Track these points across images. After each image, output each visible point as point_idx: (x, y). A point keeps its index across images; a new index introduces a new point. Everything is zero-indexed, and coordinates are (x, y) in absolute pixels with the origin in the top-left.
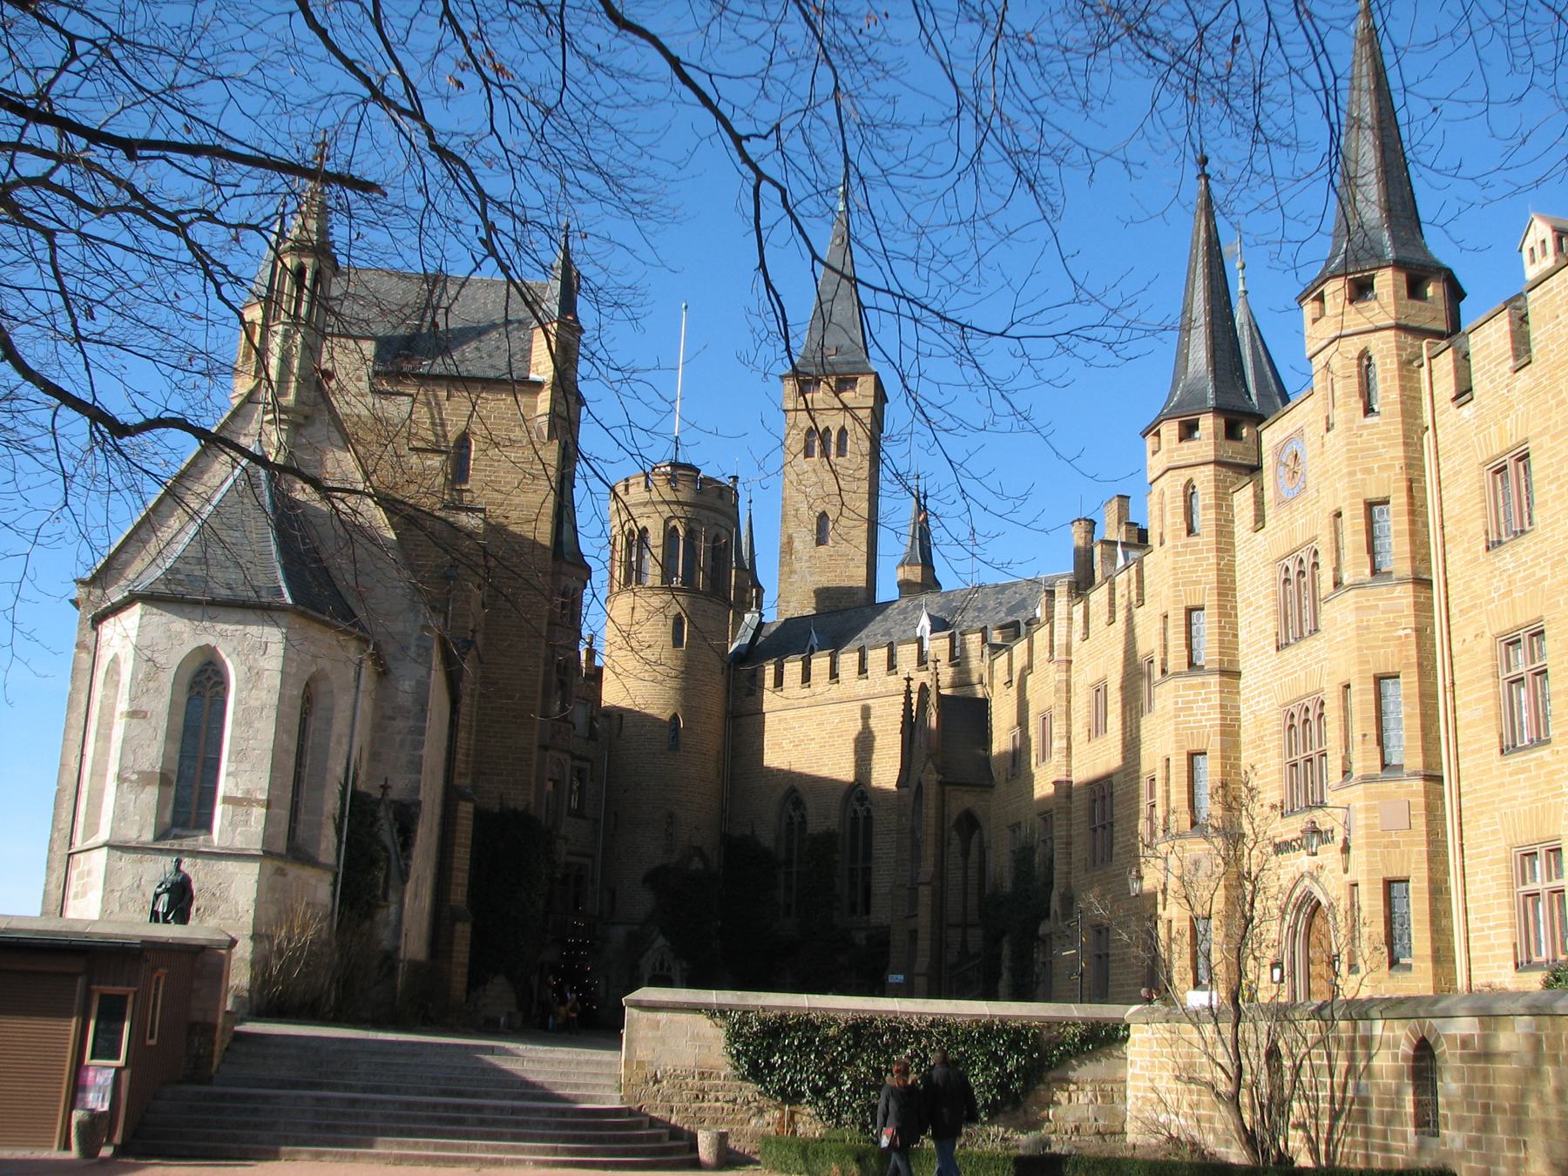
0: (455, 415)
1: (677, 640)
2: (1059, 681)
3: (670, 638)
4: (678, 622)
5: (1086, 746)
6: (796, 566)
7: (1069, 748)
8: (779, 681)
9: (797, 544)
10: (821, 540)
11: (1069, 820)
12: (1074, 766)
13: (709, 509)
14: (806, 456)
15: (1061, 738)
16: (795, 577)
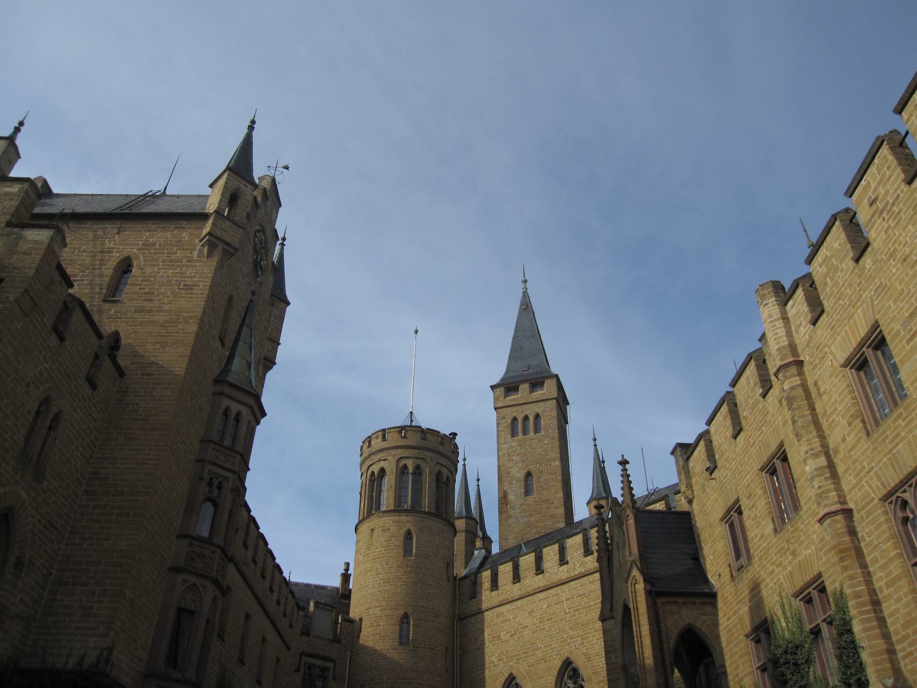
0: (122, 244)
1: (407, 551)
2: (792, 388)
3: (401, 550)
4: (408, 535)
5: (864, 445)
6: (512, 512)
7: (831, 466)
8: (495, 585)
9: (511, 497)
10: (527, 492)
11: (864, 566)
12: (845, 487)
13: (433, 451)
14: (513, 436)
15: (816, 456)
16: (510, 521)
